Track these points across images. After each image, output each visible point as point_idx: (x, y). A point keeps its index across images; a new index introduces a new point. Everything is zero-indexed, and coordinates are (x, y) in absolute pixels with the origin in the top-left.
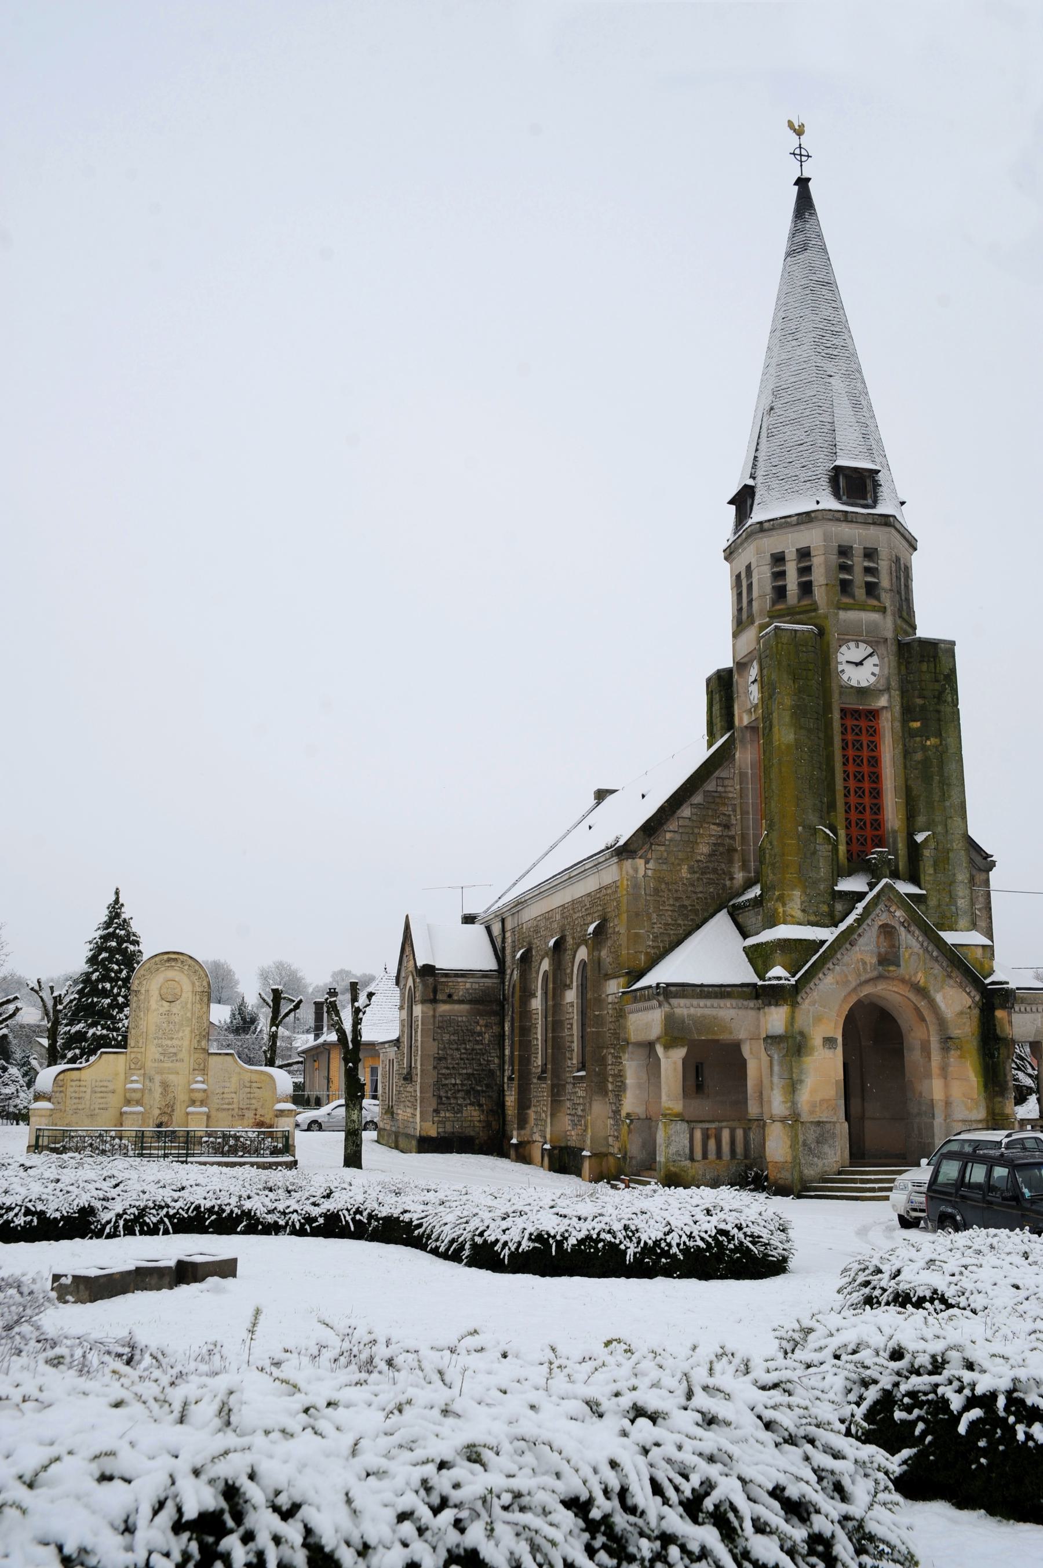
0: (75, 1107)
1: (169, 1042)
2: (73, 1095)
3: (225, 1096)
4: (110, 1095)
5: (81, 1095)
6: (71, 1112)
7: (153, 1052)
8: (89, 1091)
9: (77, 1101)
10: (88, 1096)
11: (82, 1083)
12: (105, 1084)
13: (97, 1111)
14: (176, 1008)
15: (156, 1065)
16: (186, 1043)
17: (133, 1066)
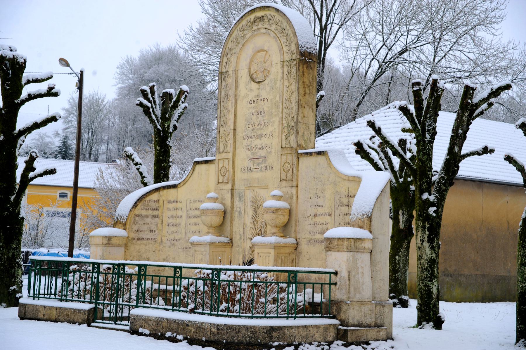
0: (172, 237)
1: (257, 142)
2: (171, 221)
3: (318, 220)
6: (168, 244)
7: (243, 158)
9: (174, 229)
11: (179, 205)
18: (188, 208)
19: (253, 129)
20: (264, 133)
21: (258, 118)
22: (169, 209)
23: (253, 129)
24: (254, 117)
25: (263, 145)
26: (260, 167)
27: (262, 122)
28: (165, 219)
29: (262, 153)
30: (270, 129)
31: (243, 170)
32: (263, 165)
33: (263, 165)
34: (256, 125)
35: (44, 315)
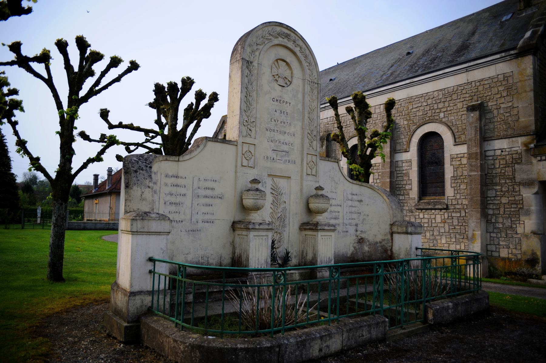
2: (168, 198)
4: (217, 201)
5: (179, 199)
8: (189, 194)
10: (187, 201)
11: (180, 181)
13: (200, 225)
14: (287, 94)
15: (269, 164)
16: (297, 141)
17: (245, 163)
18: (195, 186)
19: (276, 125)
20: (287, 132)
21: (281, 116)
22: (166, 185)
23: (276, 125)
24: (277, 114)
25: (286, 141)
26: (284, 159)
28: (162, 195)
30: (292, 130)
31: (266, 158)
32: (287, 158)
33: (287, 158)
34: (279, 122)
35: (321, 350)
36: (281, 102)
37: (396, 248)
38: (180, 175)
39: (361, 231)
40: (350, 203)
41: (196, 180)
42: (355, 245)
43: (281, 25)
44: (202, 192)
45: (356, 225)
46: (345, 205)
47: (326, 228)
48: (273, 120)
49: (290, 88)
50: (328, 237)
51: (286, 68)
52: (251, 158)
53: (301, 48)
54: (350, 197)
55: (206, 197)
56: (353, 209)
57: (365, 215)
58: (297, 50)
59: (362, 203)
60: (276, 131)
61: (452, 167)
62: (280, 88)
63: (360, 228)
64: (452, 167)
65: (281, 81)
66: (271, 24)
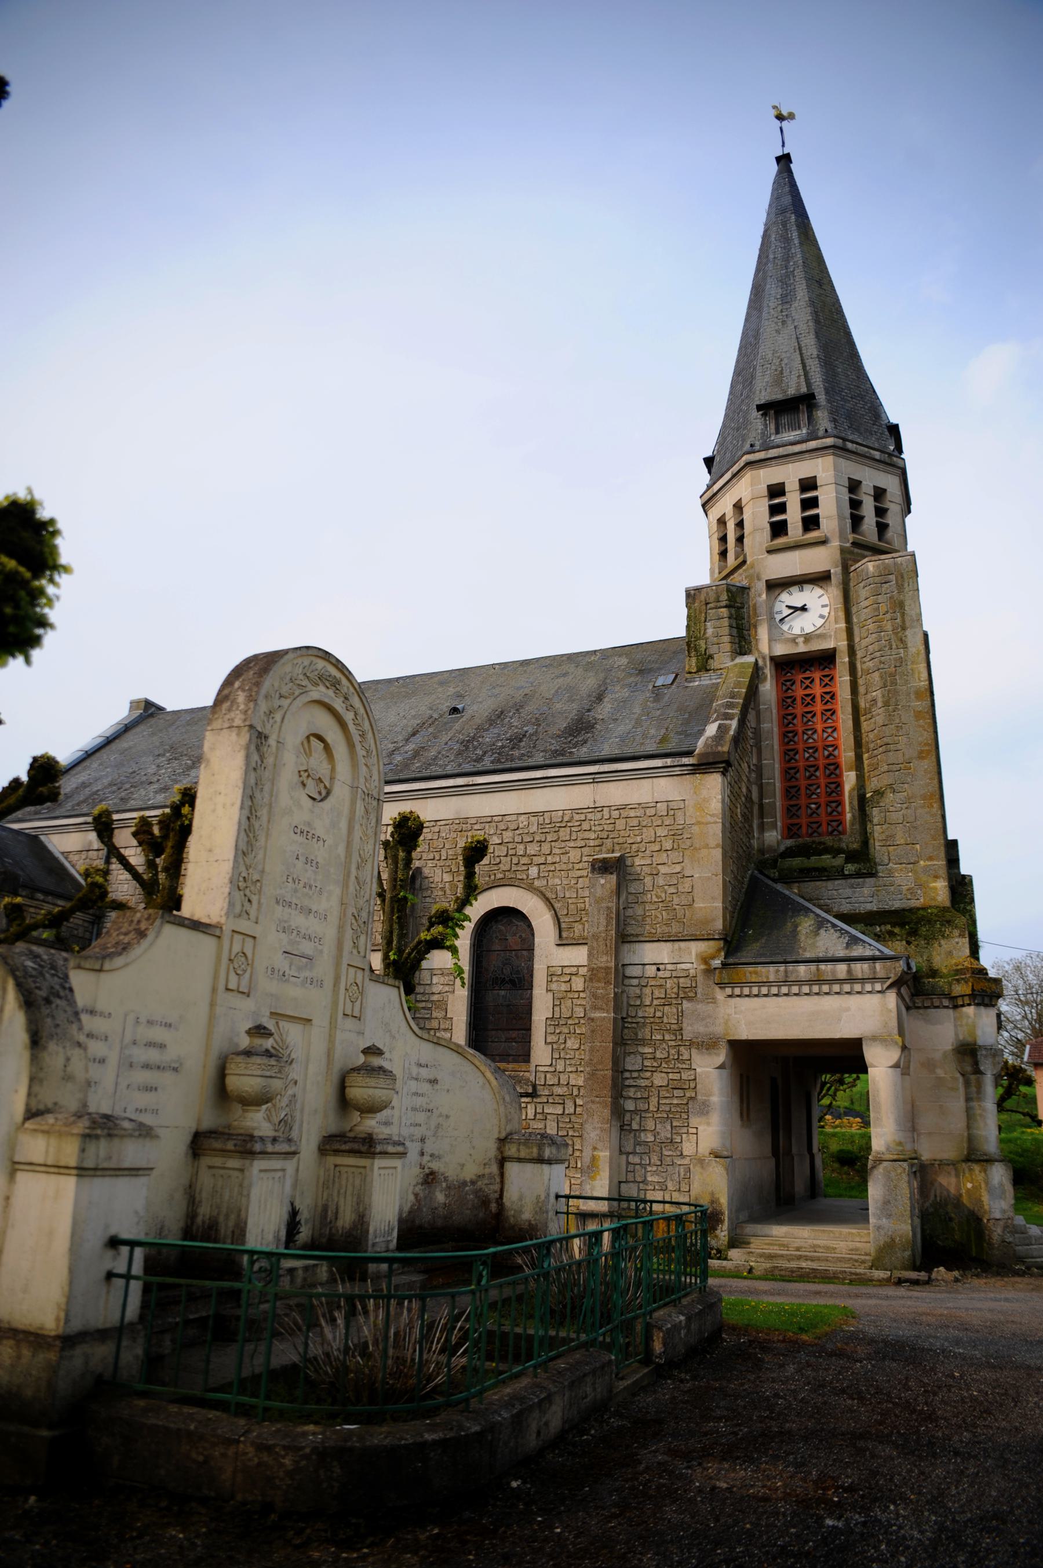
1: (299, 921)
12: (158, 1034)
16: (330, 933)
18: (128, 1038)
19: (296, 891)
20: (314, 908)
21: (306, 871)
23: (296, 891)
27: (312, 882)
29: (307, 948)
31: (269, 972)
36: (310, 835)
37: (511, 1195)
38: (100, 1006)
39: (432, 1155)
40: (413, 1085)
41: (131, 1019)
42: (417, 1189)
43: (326, 656)
44: (142, 1055)
45: (423, 1140)
46: (405, 1090)
47: (391, 1149)
48: (290, 880)
49: (326, 805)
50: (391, 1171)
51: (324, 756)
52: (245, 971)
53: (356, 714)
54: (415, 1070)
55: (147, 1066)
56: (419, 1101)
57: (440, 1115)
58: (348, 717)
59: (437, 1087)
60: (294, 906)
61: (550, 995)
62: (310, 801)
63: (429, 1147)
64: (550, 995)
65: (312, 788)
66: (310, 652)
